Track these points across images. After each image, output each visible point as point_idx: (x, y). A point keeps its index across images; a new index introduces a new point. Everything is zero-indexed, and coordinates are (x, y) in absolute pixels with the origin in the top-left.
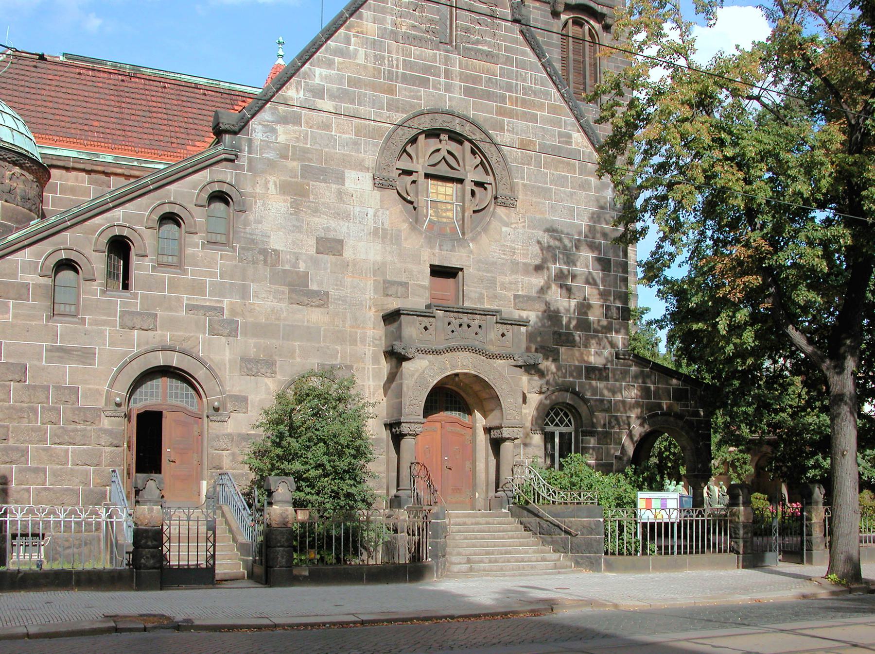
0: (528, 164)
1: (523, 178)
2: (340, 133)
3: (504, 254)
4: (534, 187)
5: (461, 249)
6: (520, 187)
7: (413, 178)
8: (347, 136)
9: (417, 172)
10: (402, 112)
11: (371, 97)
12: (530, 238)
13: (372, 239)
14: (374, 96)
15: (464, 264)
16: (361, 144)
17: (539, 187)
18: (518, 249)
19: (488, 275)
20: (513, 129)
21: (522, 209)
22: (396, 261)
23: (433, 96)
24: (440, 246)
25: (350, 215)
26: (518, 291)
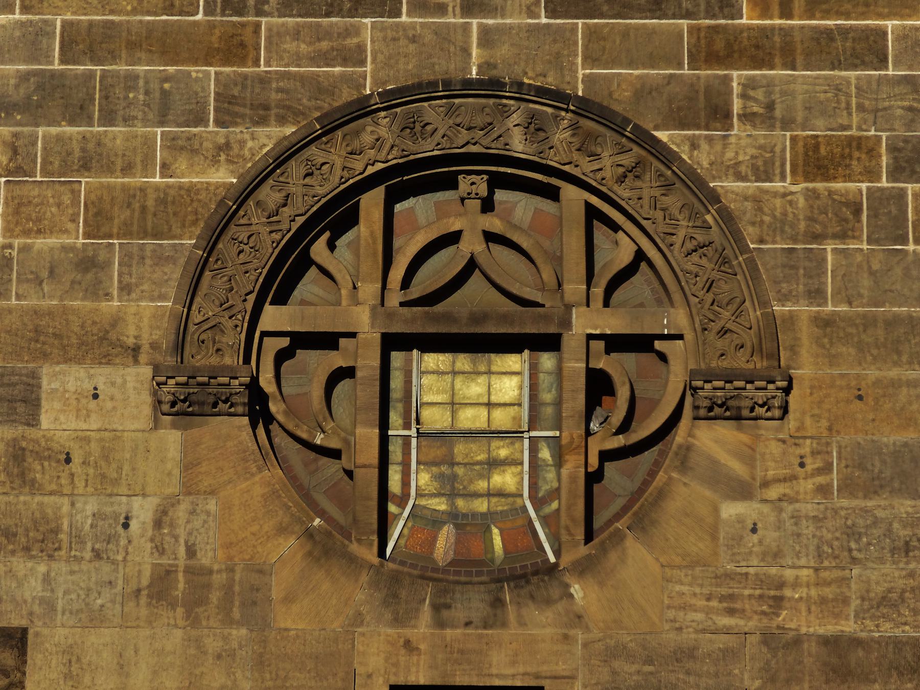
0: (842, 236)
1: (816, 295)
2: (27, 233)
3: (731, 612)
4: (869, 322)
5: (533, 613)
6: (805, 332)
7: (336, 360)
8: (53, 241)
9: (353, 335)
10: (282, 121)
11: (155, 86)
12: (852, 533)
13: (144, 612)
14: (167, 79)
15: (545, 669)
16: (108, 264)
17: (892, 322)
18: (796, 585)
20: (770, 107)
21: (816, 417)
23: (414, 40)
24: (437, 608)
25: (56, 531)
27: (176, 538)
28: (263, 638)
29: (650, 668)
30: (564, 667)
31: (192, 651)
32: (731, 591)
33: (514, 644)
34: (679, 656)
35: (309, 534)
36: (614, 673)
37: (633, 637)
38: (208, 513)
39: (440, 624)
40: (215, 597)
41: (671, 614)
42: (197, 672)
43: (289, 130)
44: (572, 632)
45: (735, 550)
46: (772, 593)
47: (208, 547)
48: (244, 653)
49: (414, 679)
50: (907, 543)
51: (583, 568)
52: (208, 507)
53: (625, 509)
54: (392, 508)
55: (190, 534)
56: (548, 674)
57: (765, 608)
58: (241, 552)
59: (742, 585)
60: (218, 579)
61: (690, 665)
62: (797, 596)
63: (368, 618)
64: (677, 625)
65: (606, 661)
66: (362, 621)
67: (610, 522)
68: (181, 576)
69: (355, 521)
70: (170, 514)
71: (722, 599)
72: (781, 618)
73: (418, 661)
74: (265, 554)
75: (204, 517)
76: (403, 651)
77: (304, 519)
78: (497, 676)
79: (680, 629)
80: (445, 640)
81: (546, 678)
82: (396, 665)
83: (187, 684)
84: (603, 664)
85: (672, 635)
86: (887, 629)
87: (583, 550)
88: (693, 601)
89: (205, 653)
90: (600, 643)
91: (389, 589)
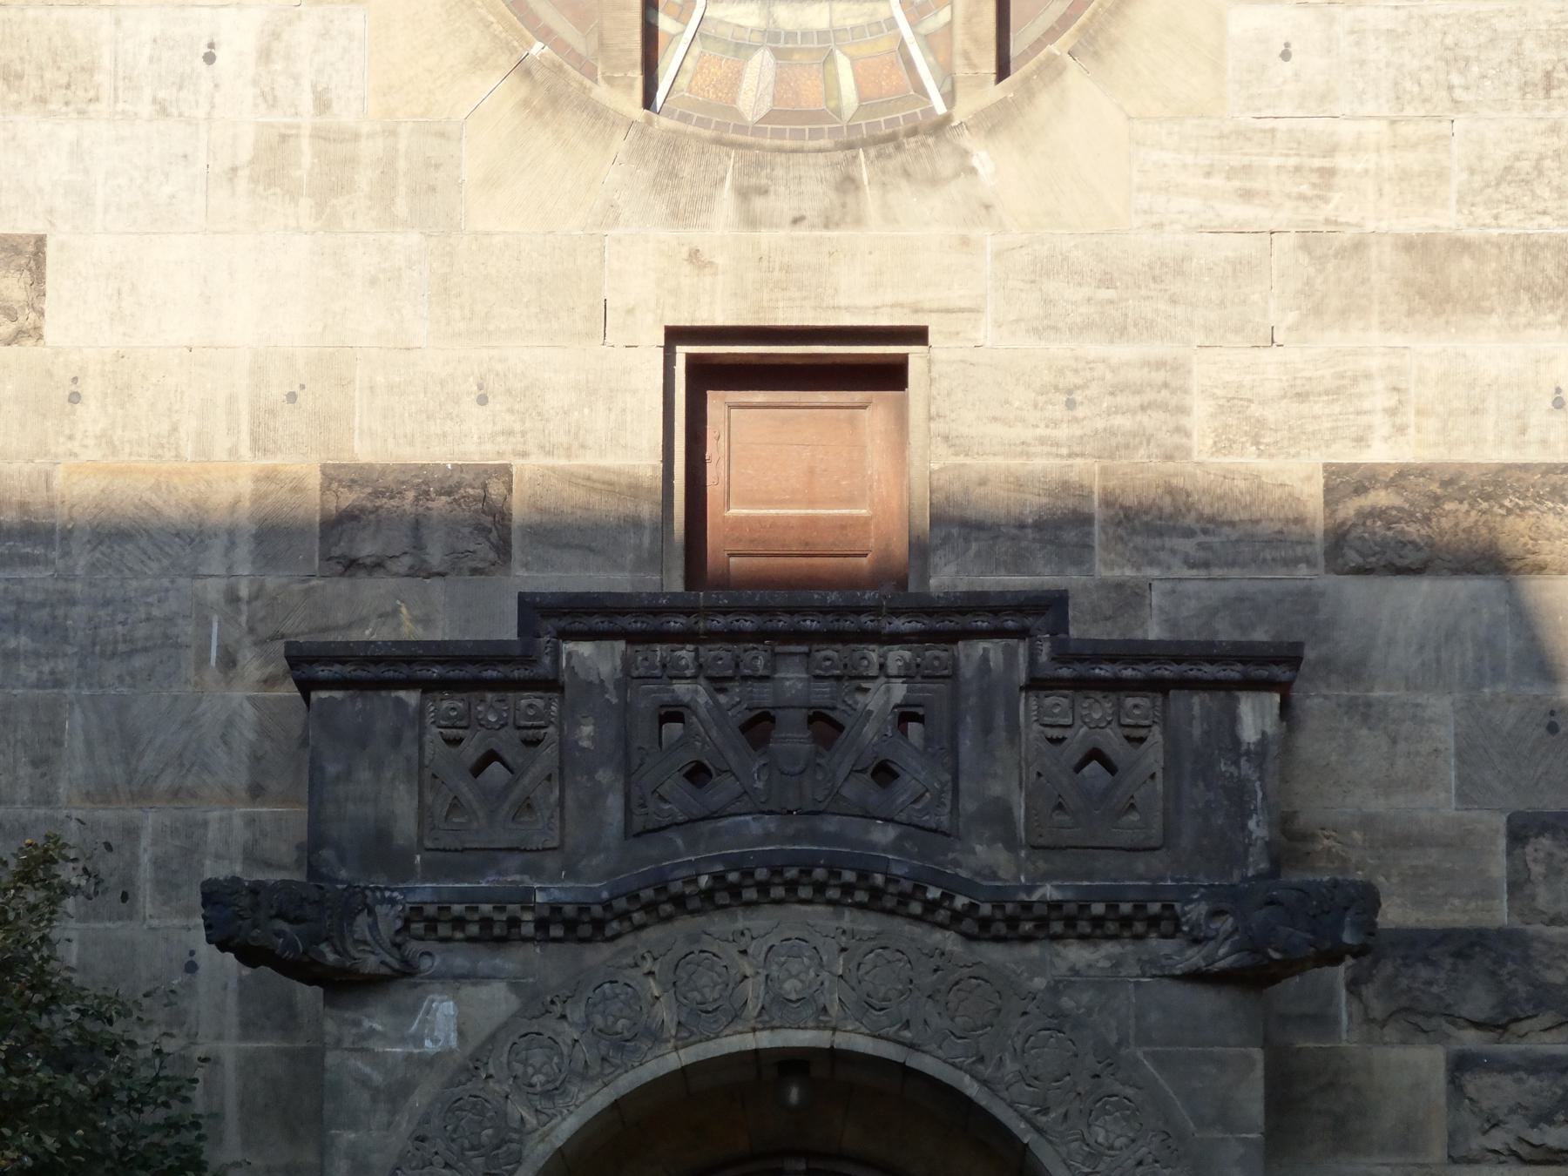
3: (1247, 195)
12: (1454, 58)
18: (1357, 148)
19: (1123, 352)
25: (89, 70)
26: (1360, 440)
27: (296, 78)
28: (448, 249)
29: (1110, 294)
32: (1246, 161)
34: (1157, 272)
35: (523, 69)
36: (1048, 302)
39: (751, 222)
40: (364, 178)
46: (1317, 163)
50: (1548, 75)
51: (994, 122)
53: (1064, 22)
54: (665, 23)
56: (935, 305)
57: (1305, 188)
62: (1359, 167)
64: (1155, 219)
65: (1033, 282)
66: (617, 218)
67: (1038, 45)
68: (305, 144)
69: (602, 45)
71: (1231, 173)
72: (1332, 205)
76: (687, 268)
77: (516, 44)
78: (847, 308)
79: (1160, 225)
81: (931, 311)
86: (1514, 223)
87: (996, 93)
91: (662, 161)
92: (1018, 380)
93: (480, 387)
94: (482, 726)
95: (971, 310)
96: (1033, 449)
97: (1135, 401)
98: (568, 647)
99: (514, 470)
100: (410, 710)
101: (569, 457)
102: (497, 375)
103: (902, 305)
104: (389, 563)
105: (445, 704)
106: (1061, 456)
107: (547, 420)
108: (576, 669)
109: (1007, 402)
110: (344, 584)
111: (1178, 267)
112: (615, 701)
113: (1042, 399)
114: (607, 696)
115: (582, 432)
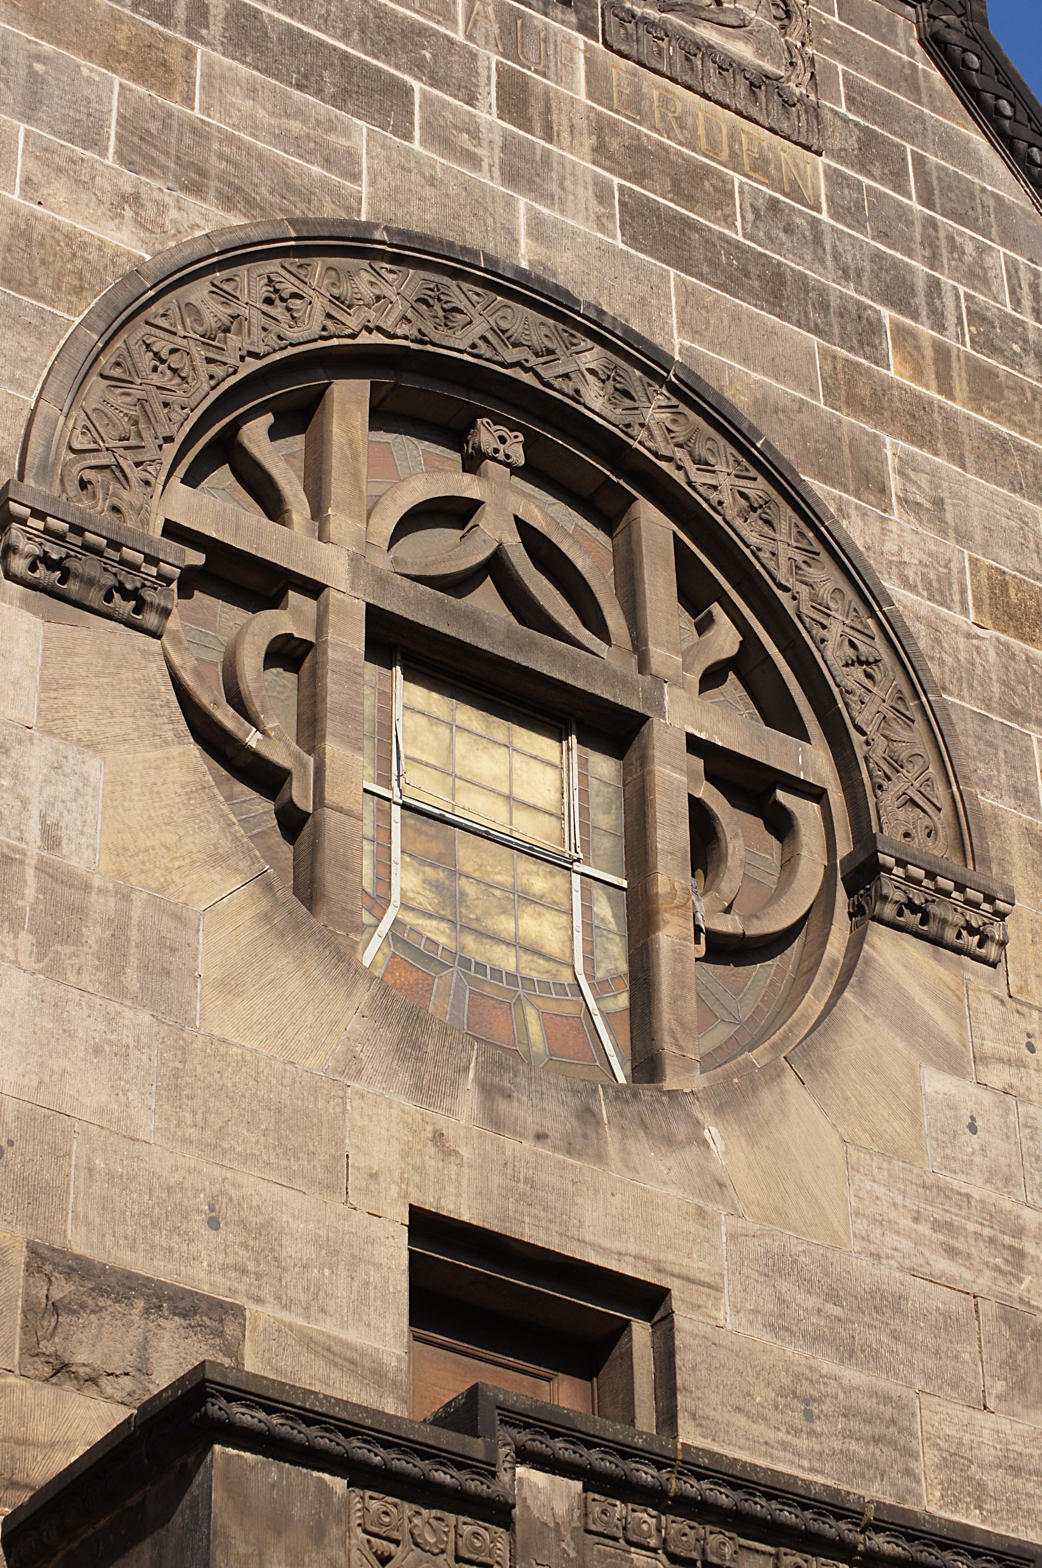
3: (952, 1252)
10: (227, 202)
14: (38, 57)
19: (853, 1375)
22: (147, 1124)
24: (489, 1091)
27: (24, 802)
28: (181, 1042)
29: (837, 1311)
30: (701, 1265)
31: (46, 1022)
32: (947, 1217)
33: (618, 1197)
34: (878, 1302)
37: (805, 1246)
38: (85, 780)
39: (496, 1123)
40: (94, 935)
41: (862, 1226)
42: (56, 1064)
43: (236, 220)
44: (710, 1207)
45: (948, 1151)
46: (1008, 1240)
47: (83, 840)
48: (145, 1058)
49: (451, 1207)
52: (85, 768)
55: (50, 804)
56: (677, 1270)
57: (999, 1261)
58: (143, 872)
59: (963, 1213)
60: (101, 905)
61: (895, 1323)
63: (368, 1071)
64: (872, 1248)
65: (766, 1275)
66: (360, 1071)
68: (30, 874)
70: (14, 754)
72: (1023, 1287)
73: (458, 1175)
74: (187, 889)
75: (75, 782)
76: (431, 1150)
77: (257, 853)
78: (592, 1245)
79: (876, 1256)
80: (504, 1153)
81: (673, 1275)
82: (420, 1170)
83: (35, 1084)
84: (762, 1279)
85: (866, 1262)
88: (893, 1215)
89: (72, 1035)
90: (756, 1241)
91: (405, 1029)
92: (758, 1374)
93: (212, 1210)
94: (417, 1544)
95: (710, 1286)
96: (775, 1452)
97: (867, 1430)
98: (521, 1471)
99: (247, 1313)
100: (335, 1500)
101: (308, 1318)
102: (231, 1200)
103: (644, 1259)
104: (104, 1381)
105: (375, 1505)
106: (803, 1468)
107: (284, 1269)
108: (529, 1502)
109: (749, 1394)
110: (48, 1393)
111: (896, 1303)
112: (573, 1554)
113: (781, 1401)
114: (563, 1545)
115: (322, 1294)
